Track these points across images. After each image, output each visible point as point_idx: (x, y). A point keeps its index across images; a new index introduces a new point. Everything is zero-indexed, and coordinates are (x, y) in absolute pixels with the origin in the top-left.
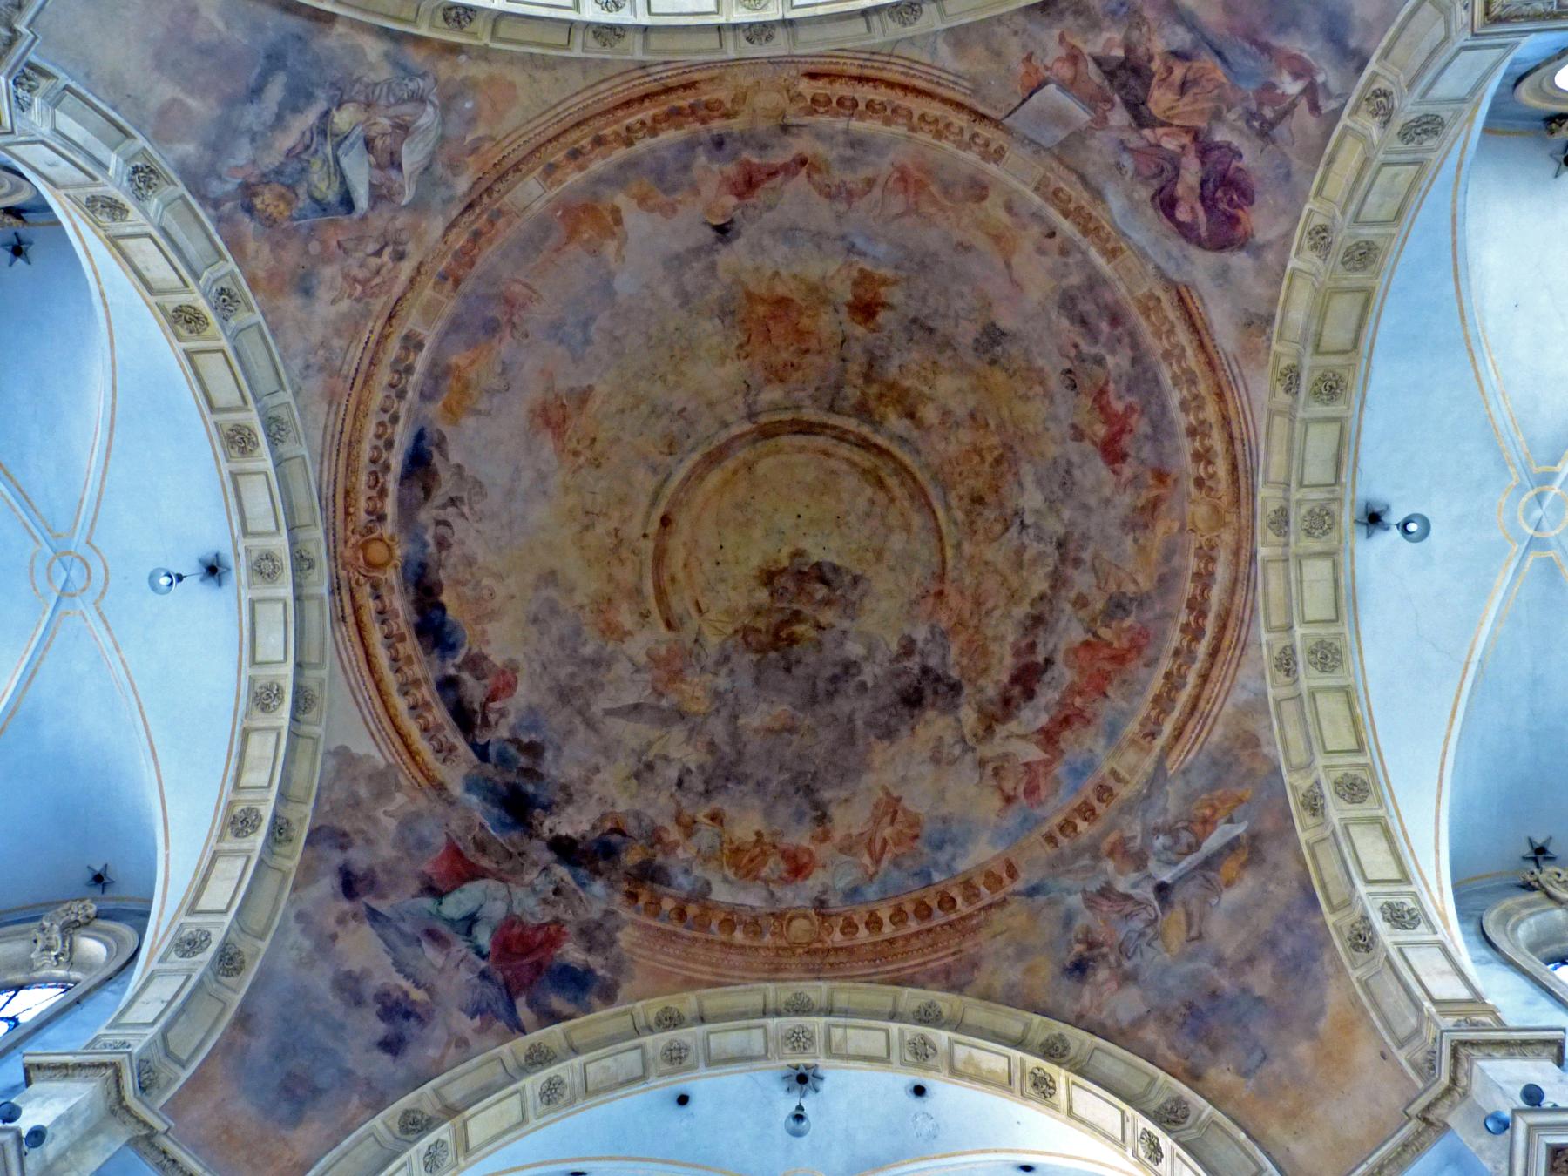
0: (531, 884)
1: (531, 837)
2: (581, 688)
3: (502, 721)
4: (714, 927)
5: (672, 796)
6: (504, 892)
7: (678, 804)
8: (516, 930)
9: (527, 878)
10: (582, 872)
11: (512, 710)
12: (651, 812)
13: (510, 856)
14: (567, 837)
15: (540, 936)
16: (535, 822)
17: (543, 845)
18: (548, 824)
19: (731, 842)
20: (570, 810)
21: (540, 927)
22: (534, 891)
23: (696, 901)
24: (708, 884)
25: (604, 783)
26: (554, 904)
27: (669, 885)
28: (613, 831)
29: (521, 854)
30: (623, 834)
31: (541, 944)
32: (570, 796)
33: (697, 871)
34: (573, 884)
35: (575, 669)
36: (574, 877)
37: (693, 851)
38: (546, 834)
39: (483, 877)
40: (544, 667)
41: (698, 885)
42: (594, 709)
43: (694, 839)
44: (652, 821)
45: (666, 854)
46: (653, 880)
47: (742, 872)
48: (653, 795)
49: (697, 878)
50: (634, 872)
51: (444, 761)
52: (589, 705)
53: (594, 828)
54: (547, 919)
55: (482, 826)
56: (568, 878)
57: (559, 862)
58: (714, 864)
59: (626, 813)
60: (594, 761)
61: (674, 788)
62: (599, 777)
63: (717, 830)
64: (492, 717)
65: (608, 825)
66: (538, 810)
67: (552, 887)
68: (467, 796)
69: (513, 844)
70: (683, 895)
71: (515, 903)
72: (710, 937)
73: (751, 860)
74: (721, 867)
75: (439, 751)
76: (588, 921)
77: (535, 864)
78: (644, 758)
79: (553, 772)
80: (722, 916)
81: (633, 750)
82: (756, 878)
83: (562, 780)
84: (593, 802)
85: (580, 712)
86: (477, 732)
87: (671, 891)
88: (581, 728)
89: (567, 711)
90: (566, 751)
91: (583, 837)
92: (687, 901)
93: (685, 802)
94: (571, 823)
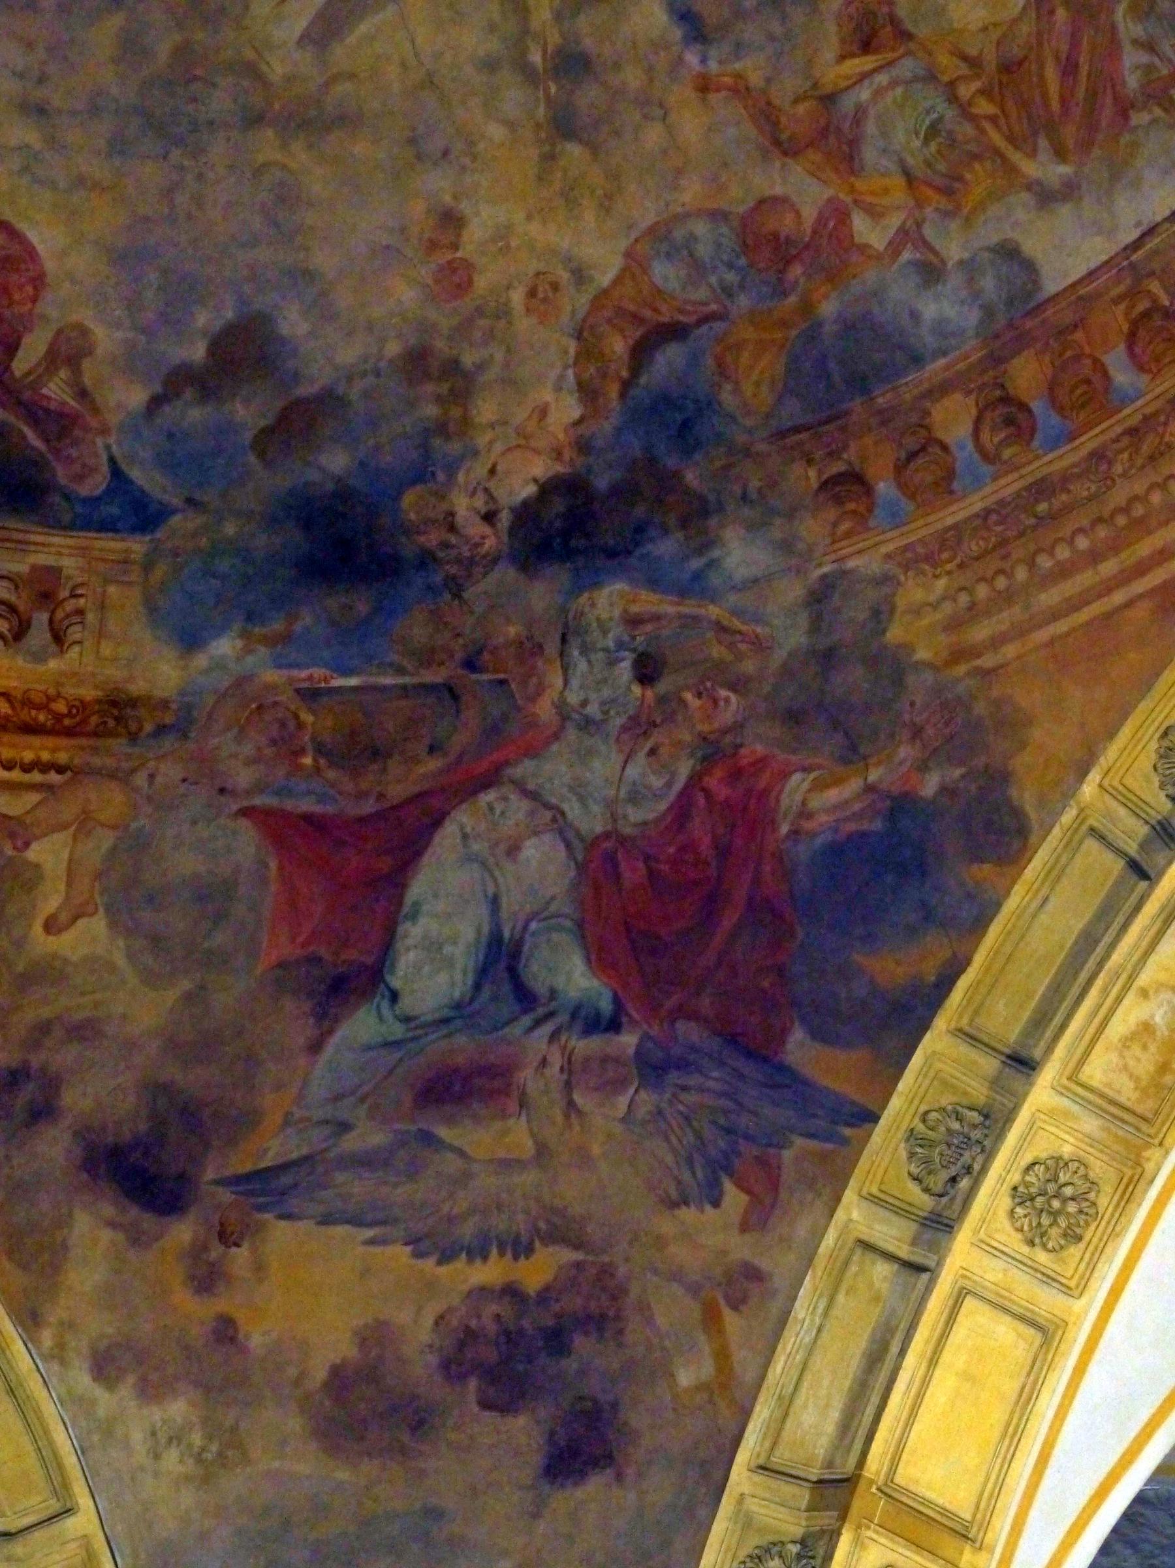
0: (563, 711)
1: (455, 586)
2: (182, 51)
3: (89, 371)
4: (1122, 376)
5: (704, 86)
6: (519, 808)
7: (740, 90)
8: (633, 874)
9: (544, 710)
10: (665, 547)
11: (85, 315)
12: (691, 192)
13: (449, 692)
14: (548, 489)
15: (700, 829)
16: (431, 539)
17: (507, 573)
18: (463, 505)
19: (974, 63)
20: (485, 409)
21: (682, 811)
22: (588, 725)
23: (1021, 341)
24: (1009, 252)
25: (502, 235)
26: (670, 707)
27: (917, 360)
28: (641, 353)
29: (471, 665)
30: (675, 332)
31: (724, 852)
32: (452, 368)
33: (953, 249)
34: (668, 607)
35: (116, 21)
36: (654, 583)
37: (899, 195)
38: (491, 541)
39: (437, 821)
40: (41, 111)
41: (988, 283)
42: (277, 70)
43: (869, 154)
44: (717, 216)
45: (834, 276)
46: (860, 384)
47: (1070, 133)
48: (654, 135)
49: (969, 267)
50: (792, 412)
51: (58, 638)
52: (252, 71)
53: (588, 393)
54: (684, 769)
55: (311, 695)
56: (648, 601)
57: (586, 582)
58: (980, 179)
59: (634, 263)
60: (418, 208)
61: (692, 59)
62: (475, 233)
63: (907, 67)
64: (57, 390)
65: (618, 346)
66: (408, 499)
67: (625, 669)
68: (201, 660)
69: (427, 657)
70: (971, 349)
71: (573, 810)
72: (1130, 415)
73: (1069, 69)
74: (1011, 170)
75: (20, 632)
76: (787, 671)
77: (528, 649)
78: (536, 57)
79: (348, 355)
80: (1119, 318)
81: (490, 65)
82: (1124, 109)
83: (393, 348)
84: (524, 324)
85: (254, 120)
86: (62, 475)
87: (935, 368)
88: (300, 155)
89: (218, 150)
90: (324, 260)
91: (584, 446)
92: (996, 360)
93: (754, 69)
94: (524, 442)
